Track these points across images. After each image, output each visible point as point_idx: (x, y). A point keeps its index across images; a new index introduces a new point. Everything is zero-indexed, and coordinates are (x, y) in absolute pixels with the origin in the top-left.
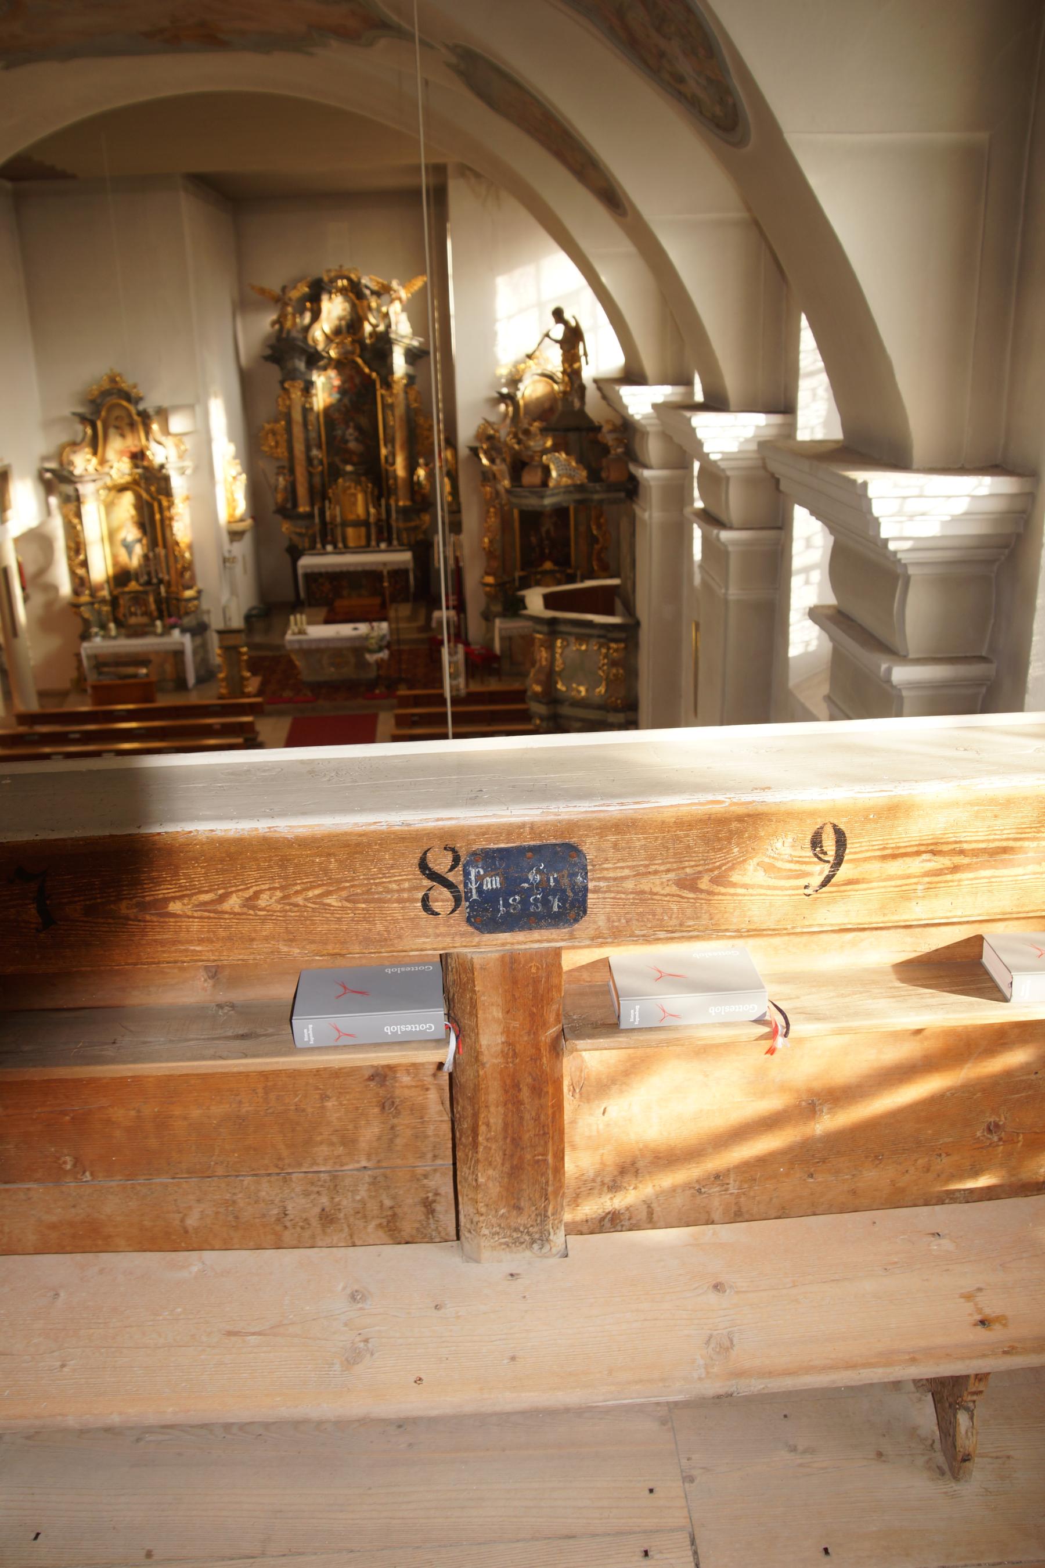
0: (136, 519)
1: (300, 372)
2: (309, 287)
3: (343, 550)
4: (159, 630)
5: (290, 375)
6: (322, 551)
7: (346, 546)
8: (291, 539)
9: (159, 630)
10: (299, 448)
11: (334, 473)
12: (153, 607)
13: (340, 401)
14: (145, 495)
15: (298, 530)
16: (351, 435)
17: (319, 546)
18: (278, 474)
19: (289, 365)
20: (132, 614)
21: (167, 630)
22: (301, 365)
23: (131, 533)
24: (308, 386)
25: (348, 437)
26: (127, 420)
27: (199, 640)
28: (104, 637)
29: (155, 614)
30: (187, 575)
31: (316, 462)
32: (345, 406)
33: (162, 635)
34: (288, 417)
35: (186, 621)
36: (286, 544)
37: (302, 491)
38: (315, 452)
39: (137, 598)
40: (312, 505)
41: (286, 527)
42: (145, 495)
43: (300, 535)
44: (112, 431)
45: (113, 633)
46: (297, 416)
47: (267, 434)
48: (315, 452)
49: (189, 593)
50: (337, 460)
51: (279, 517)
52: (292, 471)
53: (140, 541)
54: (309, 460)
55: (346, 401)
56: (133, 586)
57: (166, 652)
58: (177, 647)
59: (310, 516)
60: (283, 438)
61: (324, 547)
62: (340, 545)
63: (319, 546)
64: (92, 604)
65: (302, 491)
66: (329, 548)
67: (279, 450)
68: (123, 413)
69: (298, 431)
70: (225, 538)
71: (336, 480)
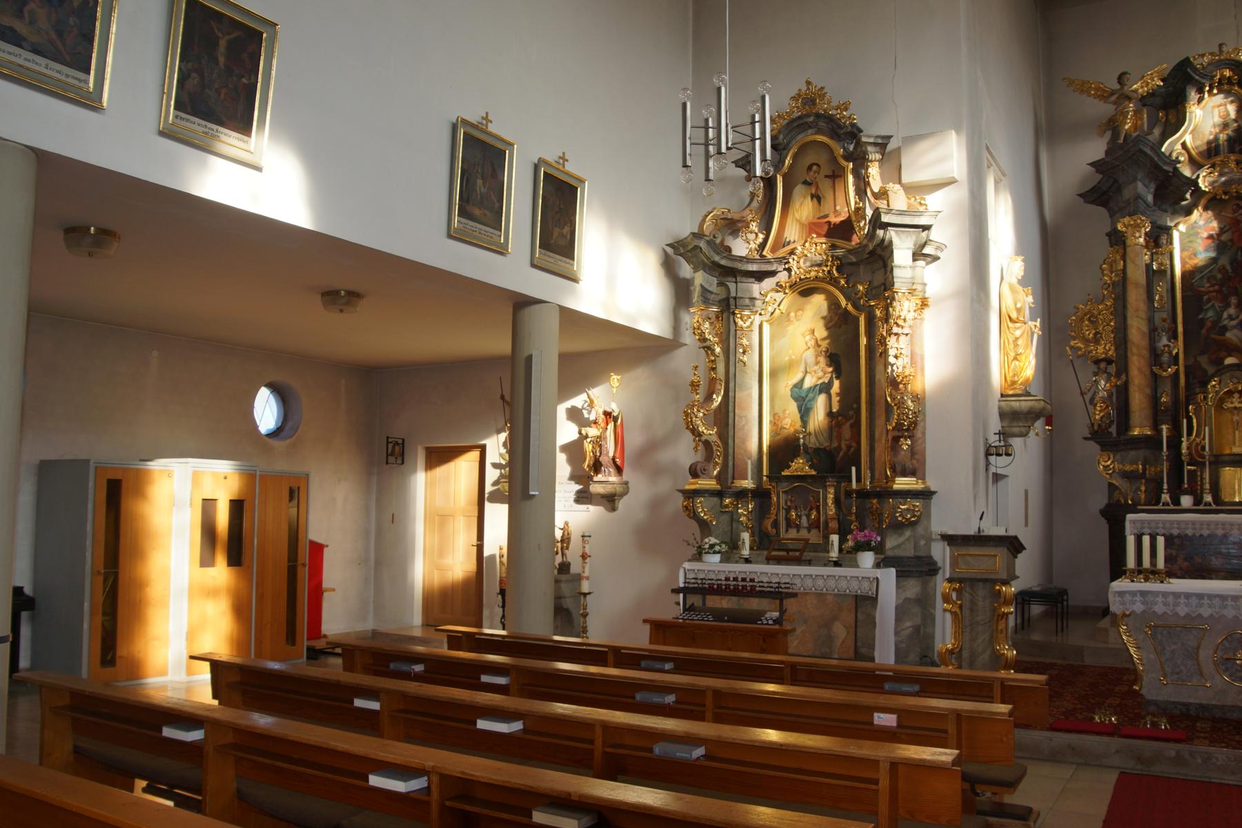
0: (825, 344)
1: (1145, 202)
2: (1162, 80)
3: (1214, 507)
4: (834, 554)
5: (1133, 208)
6: (1172, 507)
7: (1217, 499)
8: (1111, 487)
9: (834, 554)
10: (1137, 327)
11: (1198, 379)
12: (832, 511)
13: (1213, 261)
14: (843, 302)
15: (1128, 468)
16: (1231, 318)
17: (1166, 497)
18: (1096, 374)
19: (1127, 193)
20: (790, 524)
21: (847, 557)
22: (1150, 198)
23: (816, 373)
24: (1159, 237)
25: (1225, 322)
26: (826, 170)
27: (913, 588)
28: (726, 559)
29: (834, 525)
30: (905, 444)
31: (1165, 358)
32: (1222, 269)
33: (837, 564)
34: (1121, 287)
35: (891, 542)
36: (1105, 501)
37: (1138, 400)
38: (1164, 341)
39: (802, 489)
40: (1156, 427)
41: (1106, 463)
42: (843, 302)
43: (1129, 476)
44: (799, 190)
45: (746, 552)
46: (1137, 274)
47: (1082, 320)
48: (1164, 341)
49: (903, 483)
50: (1203, 360)
51: (1093, 447)
52: (1123, 369)
53: (825, 388)
54: (1155, 356)
55: (1224, 261)
56: (800, 466)
57: (842, 596)
58: (866, 588)
59: (1152, 442)
60: (1108, 326)
61: (1176, 502)
62: (1208, 498)
63: (1166, 497)
64: (720, 494)
65: (1138, 400)
66: (1186, 501)
67: (1101, 349)
68: (822, 158)
69: (1136, 298)
70: (995, 424)
71: (1204, 384)
